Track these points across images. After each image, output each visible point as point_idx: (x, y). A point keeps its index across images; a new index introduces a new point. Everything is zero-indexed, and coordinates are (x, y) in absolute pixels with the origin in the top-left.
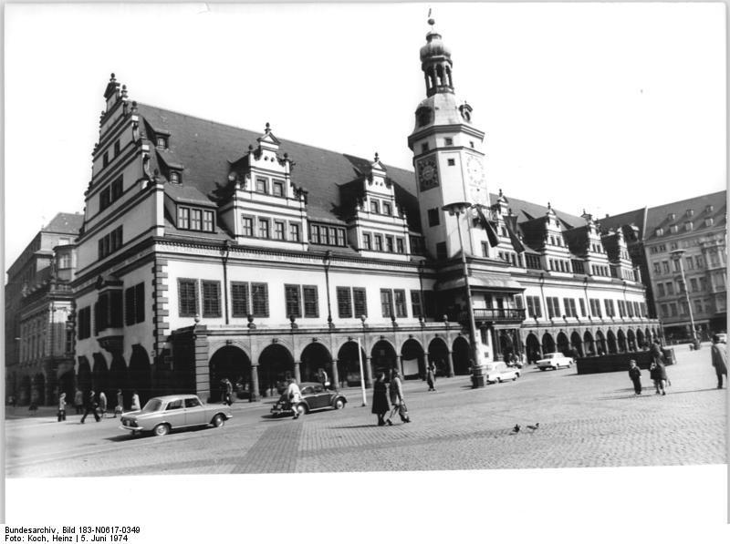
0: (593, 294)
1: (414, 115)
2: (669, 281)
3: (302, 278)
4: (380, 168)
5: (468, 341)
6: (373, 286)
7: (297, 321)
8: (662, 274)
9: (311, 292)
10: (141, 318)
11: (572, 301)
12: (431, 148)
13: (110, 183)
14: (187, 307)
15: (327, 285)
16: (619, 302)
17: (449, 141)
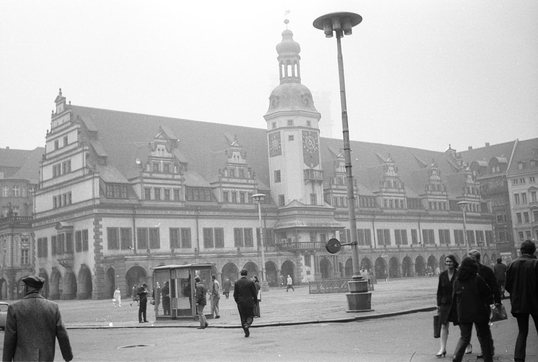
0: (425, 226)
1: (269, 100)
2: (525, 211)
3: (180, 224)
4: (237, 145)
5: (295, 263)
6: (229, 228)
7: (176, 250)
8: (521, 204)
9: (186, 232)
10: (86, 248)
11: (404, 232)
12: (277, 127)
13: (61, 162)
14: (112, 245)
15: (197, 227)
16: (455, 231)
17: (290, 122)
